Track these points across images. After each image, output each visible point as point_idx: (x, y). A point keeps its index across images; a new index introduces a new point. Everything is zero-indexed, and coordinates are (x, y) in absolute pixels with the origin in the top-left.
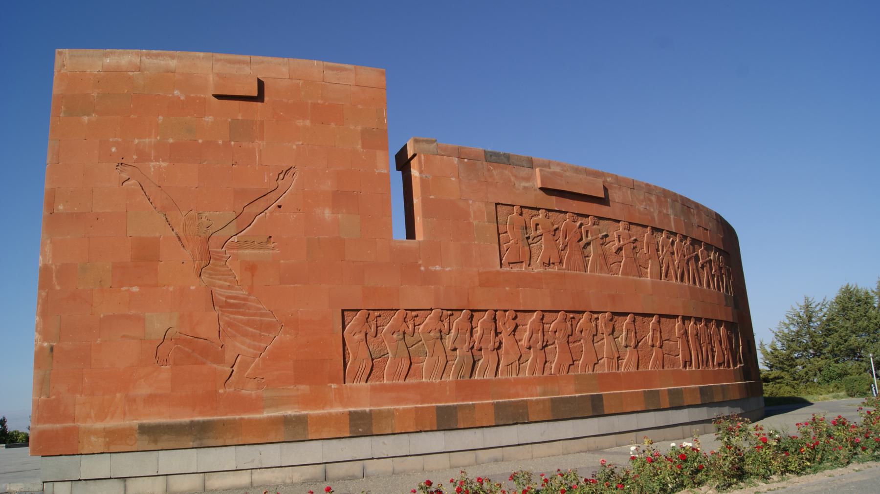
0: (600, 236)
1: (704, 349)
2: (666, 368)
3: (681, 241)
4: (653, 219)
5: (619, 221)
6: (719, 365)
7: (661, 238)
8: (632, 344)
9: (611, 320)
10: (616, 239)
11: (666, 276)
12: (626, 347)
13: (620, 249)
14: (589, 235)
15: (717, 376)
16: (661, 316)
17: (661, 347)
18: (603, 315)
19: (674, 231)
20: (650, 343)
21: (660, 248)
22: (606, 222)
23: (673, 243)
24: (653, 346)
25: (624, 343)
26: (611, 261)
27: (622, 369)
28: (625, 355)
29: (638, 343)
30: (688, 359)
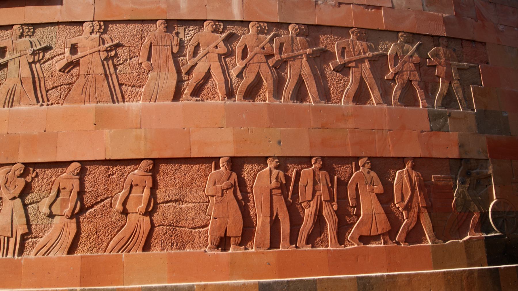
0: (30, 51)
1: (308, 213)
2: (156, 251)
3: (261, 31)
4: (177, 7)
5: (81, 23)
6: (364, 239)
7: (189, 35)
8: (67, 211)
9: (21, 176)
10: (67, 50)
11: (197, 92)
12: (51, 216)
13: (75, 64)
14: (7, 54)
15: (336, 262)
16: (157, 162)
17: (149, 213)
18: (7, 168)
19: (238, 18)
20: (118, 206)
21: (189, 49)
22: (50, 29)
23: (230, 39)
24: (125, 212)
25: (45, 210)
26: (49, 85)
27: (30, 255)
28: (44, 230)
29: (83, 209)
30: (235, 229)
